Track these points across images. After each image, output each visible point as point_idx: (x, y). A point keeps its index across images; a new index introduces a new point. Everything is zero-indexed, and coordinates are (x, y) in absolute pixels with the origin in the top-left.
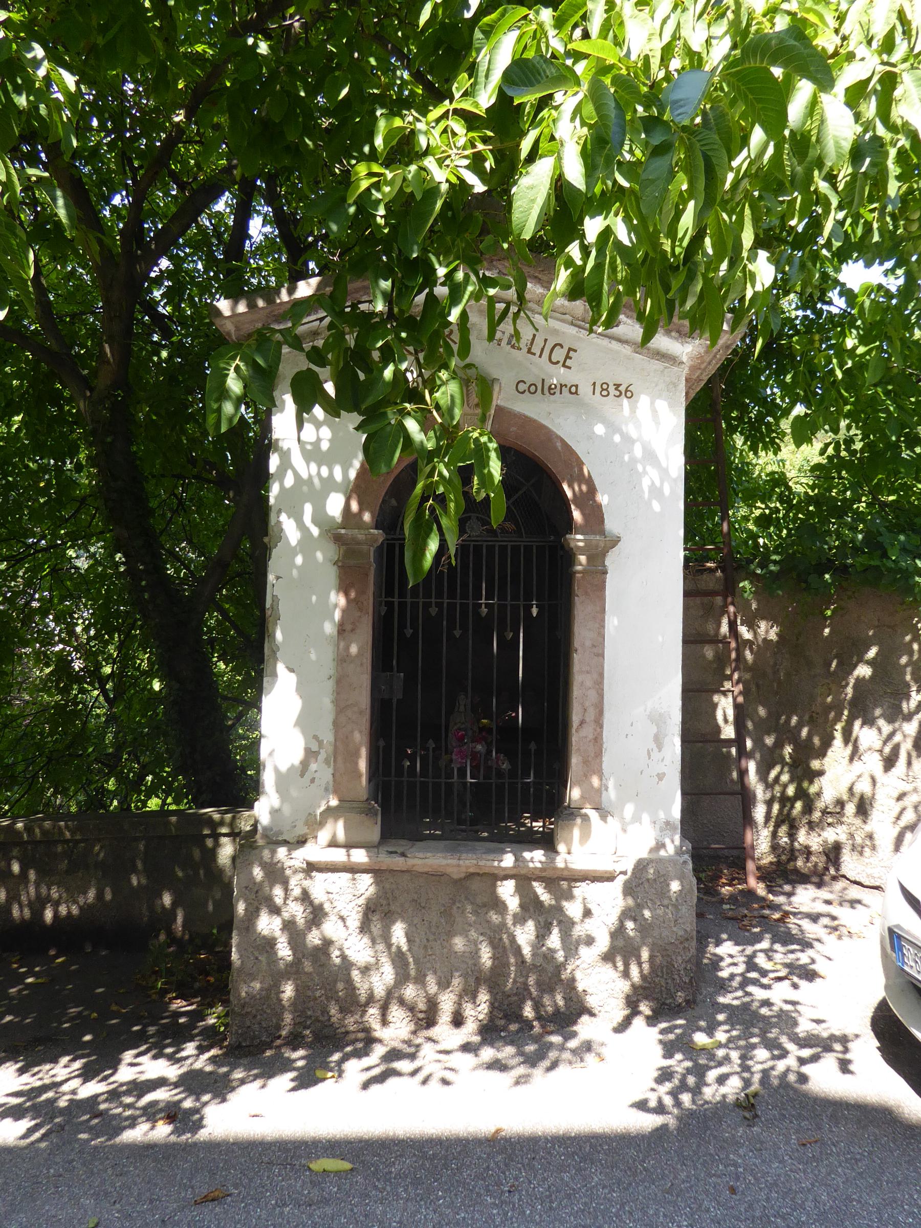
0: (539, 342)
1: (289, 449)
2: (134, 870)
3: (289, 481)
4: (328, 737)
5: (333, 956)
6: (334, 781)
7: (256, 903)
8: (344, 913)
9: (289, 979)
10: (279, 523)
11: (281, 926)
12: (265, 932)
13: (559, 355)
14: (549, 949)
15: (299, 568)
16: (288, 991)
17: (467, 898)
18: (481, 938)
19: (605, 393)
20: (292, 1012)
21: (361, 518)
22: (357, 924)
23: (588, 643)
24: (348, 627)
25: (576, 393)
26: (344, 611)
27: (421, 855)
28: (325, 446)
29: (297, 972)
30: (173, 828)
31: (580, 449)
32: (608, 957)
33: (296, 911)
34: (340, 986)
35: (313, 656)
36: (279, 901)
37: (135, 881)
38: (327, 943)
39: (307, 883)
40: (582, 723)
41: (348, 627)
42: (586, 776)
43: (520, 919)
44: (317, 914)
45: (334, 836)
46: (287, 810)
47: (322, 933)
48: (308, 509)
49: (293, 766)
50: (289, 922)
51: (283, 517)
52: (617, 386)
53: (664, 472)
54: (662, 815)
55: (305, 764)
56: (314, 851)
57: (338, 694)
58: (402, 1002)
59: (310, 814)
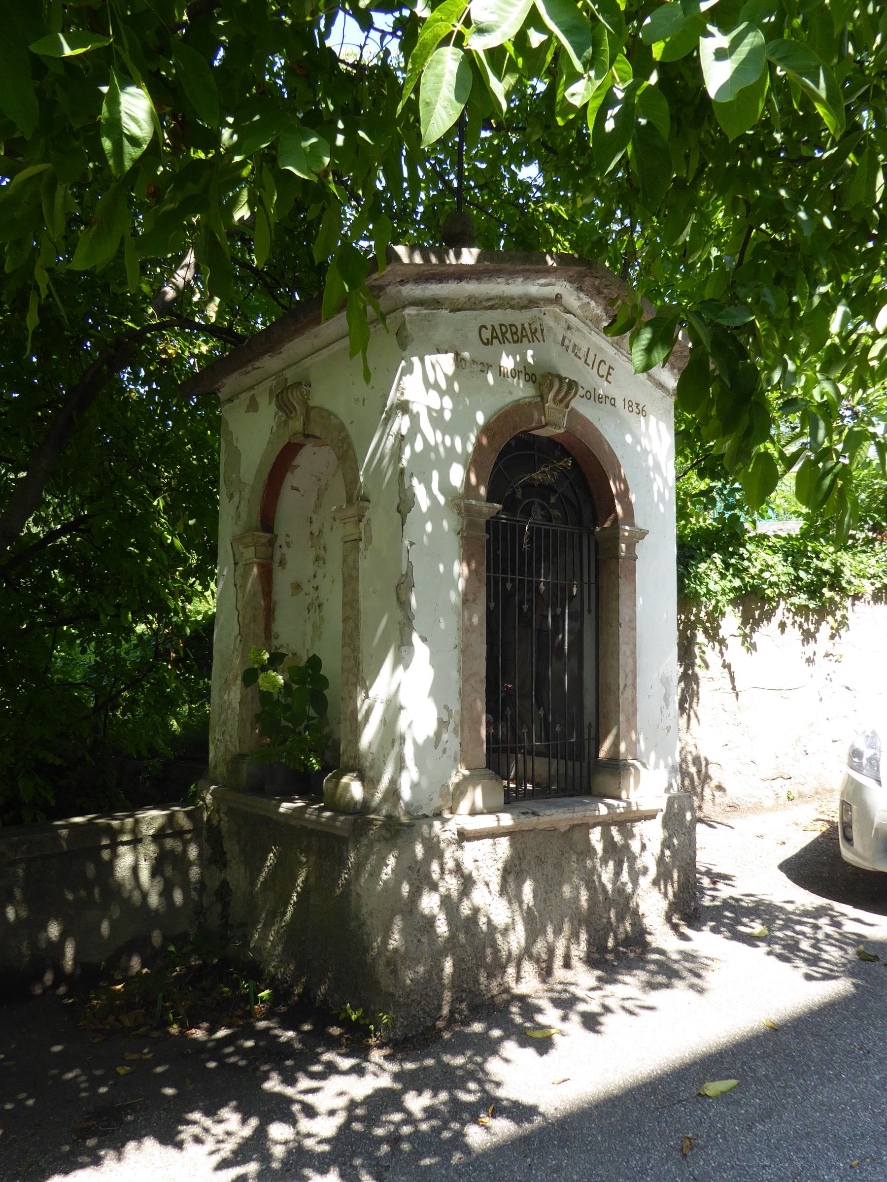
0: (592, 355)
1: (418, 413)
2: (10, 899)
3: (419, 446)
4: (455, 707)
5: (481, 923)
6: (461, 750)
7: (417, 883)
8: (487, 879)
9: (447, 956)
10: (411, 486)
11: (439, 903)
12: (426, 912)
13: (604, 370)
14: (622, 883)
15: (428, 535)
16: (448, 966)
17: (571, 848)
18: (582, 883)
19: (630, 409)
20: (450, 989)
21: (478, 491)
22: (498, 888)
23: (627, 618)
24: (471, 597)
25: (614, 405)
26: (468, 581)
27: (548, 812)
28: (447, 415)
29: (454, 947)
30: (64, 844)
31: (618, 453)
32: (655, 883)
33: (451, 884)
34: (489, 951)
35: (442, 625)
36: (435, 876)
37: (11, 913)
38: (476, 911)
39: (458, 854)
40: (625, 686)
41: (471, 597)
42: (629, 732)
43: (604, 861)
44: (467, 883)
45: (473, 804)
46: (424, 784)
47: (472, 903)
48: (435, 475)
49: (428, 737)
50: (446, 896)
51: (415, 482)
52: (638, 405)
53: (665, 480)
54: (670, 761)
55: (438, 734)
56: (462, 820)
57: (464, 662)
58: (531, 957)
59: (443, 785)
